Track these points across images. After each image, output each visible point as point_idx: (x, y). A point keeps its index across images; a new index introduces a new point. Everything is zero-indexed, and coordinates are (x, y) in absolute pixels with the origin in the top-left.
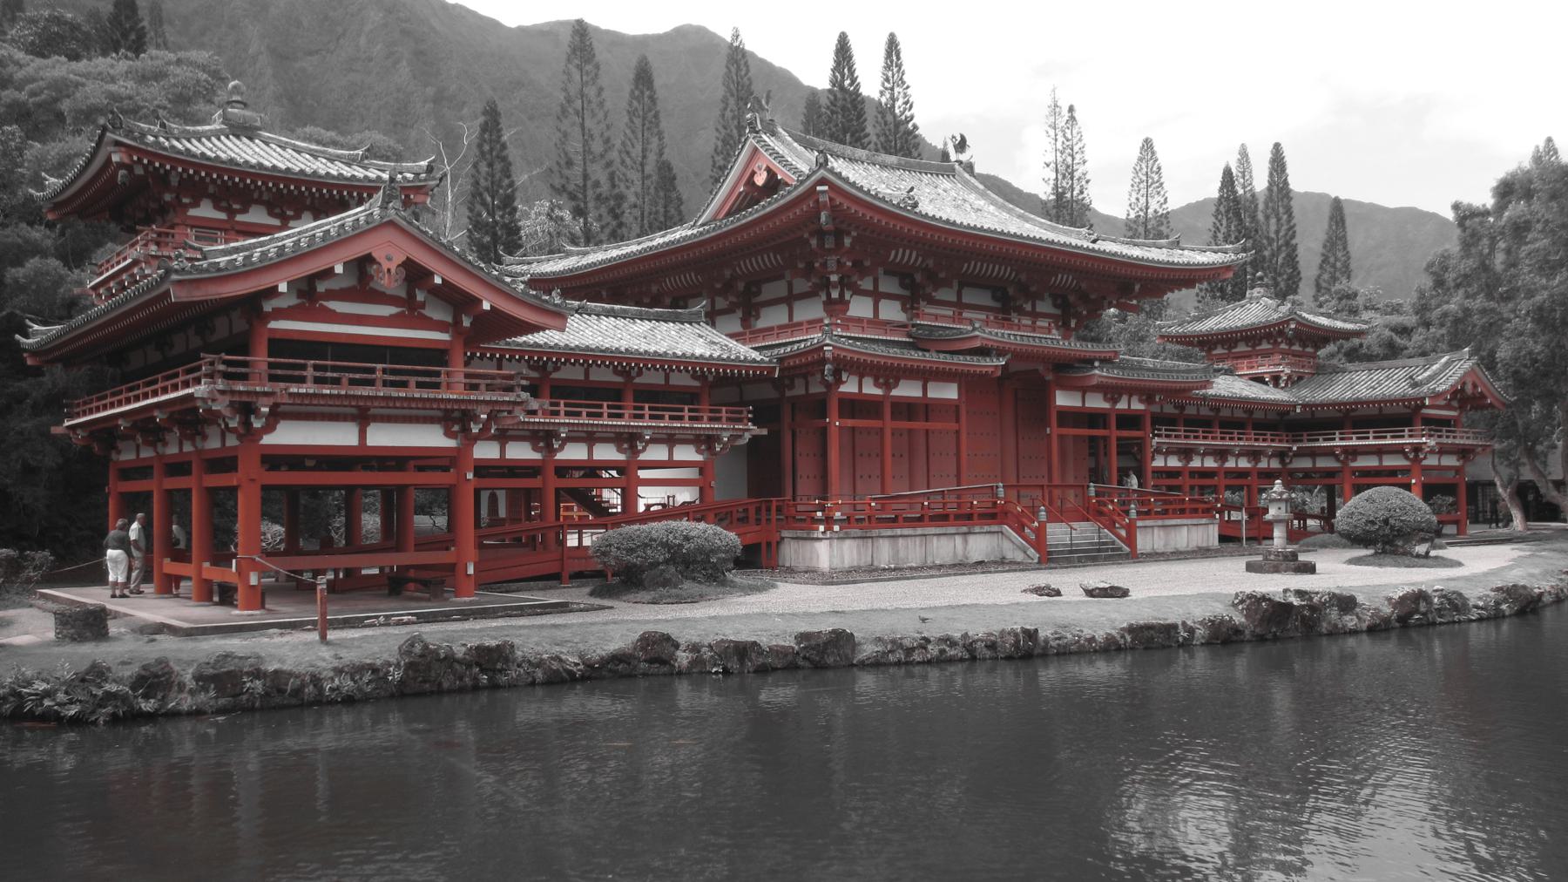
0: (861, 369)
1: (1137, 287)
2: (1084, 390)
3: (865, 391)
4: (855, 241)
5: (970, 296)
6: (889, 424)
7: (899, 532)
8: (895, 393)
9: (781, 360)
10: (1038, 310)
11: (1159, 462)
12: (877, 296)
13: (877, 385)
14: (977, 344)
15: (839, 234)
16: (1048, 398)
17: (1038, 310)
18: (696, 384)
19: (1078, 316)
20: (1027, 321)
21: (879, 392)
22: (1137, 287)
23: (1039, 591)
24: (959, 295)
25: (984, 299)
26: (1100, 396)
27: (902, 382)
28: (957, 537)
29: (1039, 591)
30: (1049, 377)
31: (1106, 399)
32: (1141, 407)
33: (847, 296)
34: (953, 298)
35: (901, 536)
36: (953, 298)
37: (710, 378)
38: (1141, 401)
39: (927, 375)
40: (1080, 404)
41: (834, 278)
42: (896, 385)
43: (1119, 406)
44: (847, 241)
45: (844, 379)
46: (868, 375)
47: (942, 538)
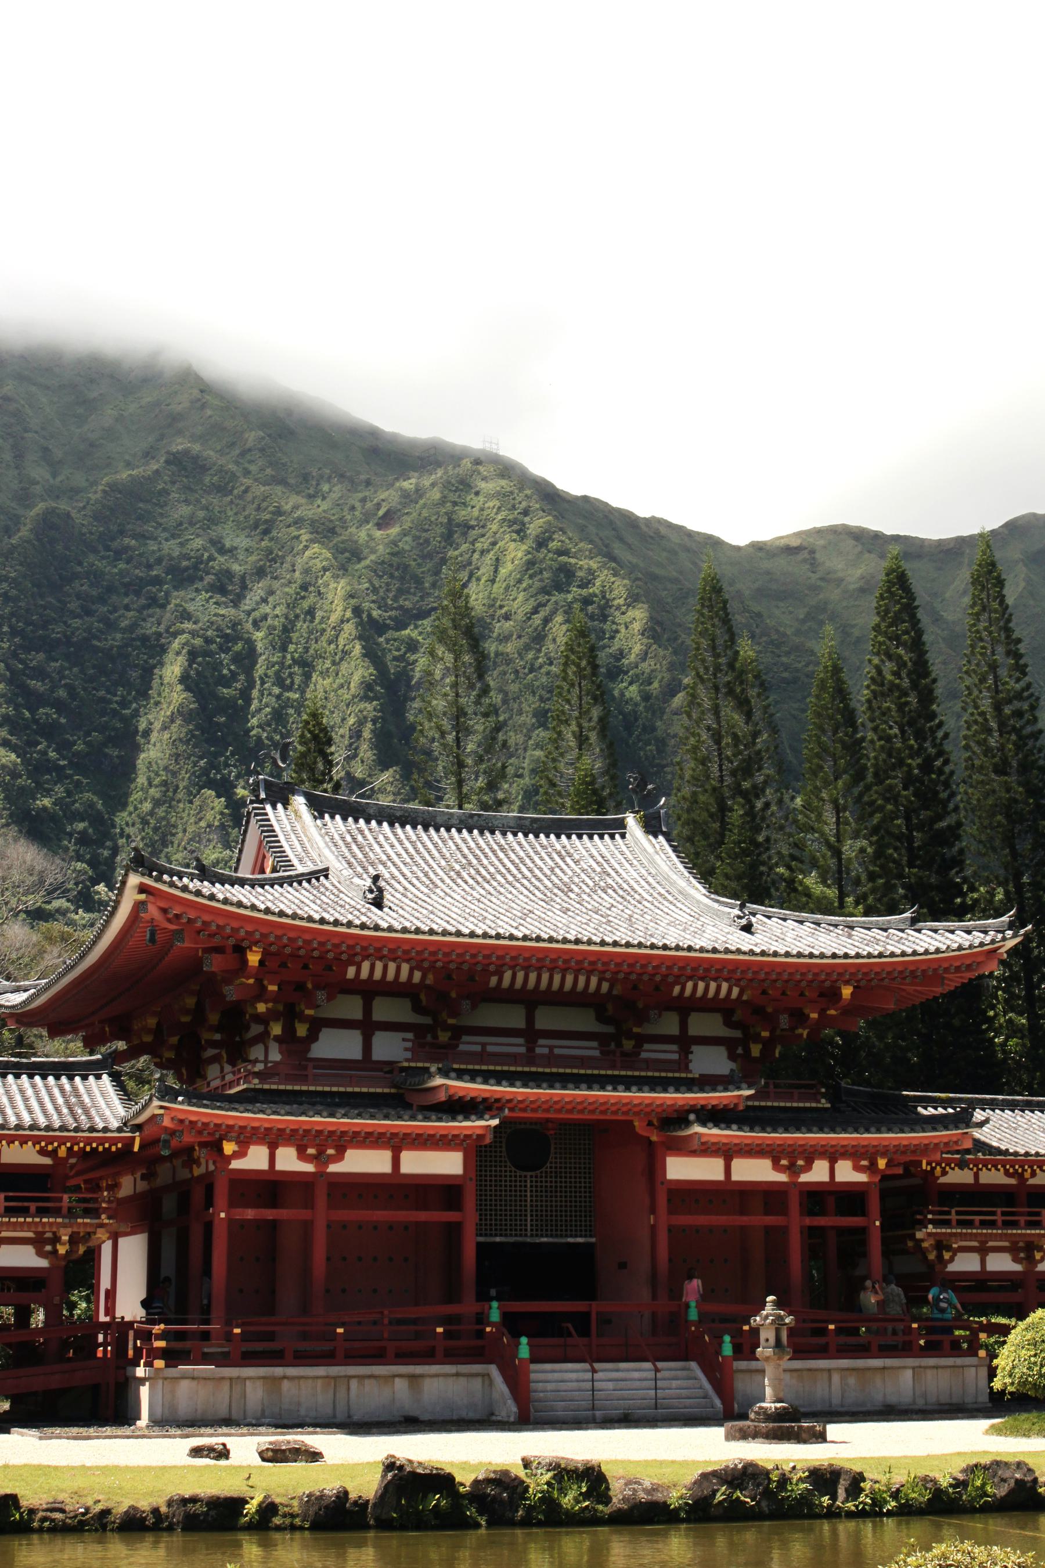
0: (273, 1139)
1: (847, 992)
2: (728, 1153)
3: (279, 1166)
4: (266, 955)
5: (545, 1019)
6: (321, 1215)
7: (279, 1371)
8: (333, 1168)
9: (138, 1127)
10: (693, 1031)
11: (966, 1263)
12: (368, 1027)
13: (302, 1156)
14: (442, 1097)
15: (240, 951)
16: (654, 1168)
17: (693, 1031)
18: (47, 1161)
19: (757, 1038)
20: (670, 1053)
21: (309, 1168)
22: (847, 992)
23: (197, 1452)
24: (530, 1019)
25: (583, 1021)
26: (767, 1163)
27: (349, 1153)
28: (397, 1380)
29: (197, 1452)
30: (654, 1138)
31: (776, 1166)
32: (862, 1178)
33: (302, 1030)
34: (520, 1023)
35: (285, 1377)
36: (520, 1023)
37: (62, 1152)
38: (857, 1168)
39: (397, 1144)
40: (720, 1176)
41: (261, 1008)
42: (339, 1157)
43: (804, 1178)
44: (254, 958)
45: (229, 1148)
46: (287, 1143)
47: (367, 1382)
